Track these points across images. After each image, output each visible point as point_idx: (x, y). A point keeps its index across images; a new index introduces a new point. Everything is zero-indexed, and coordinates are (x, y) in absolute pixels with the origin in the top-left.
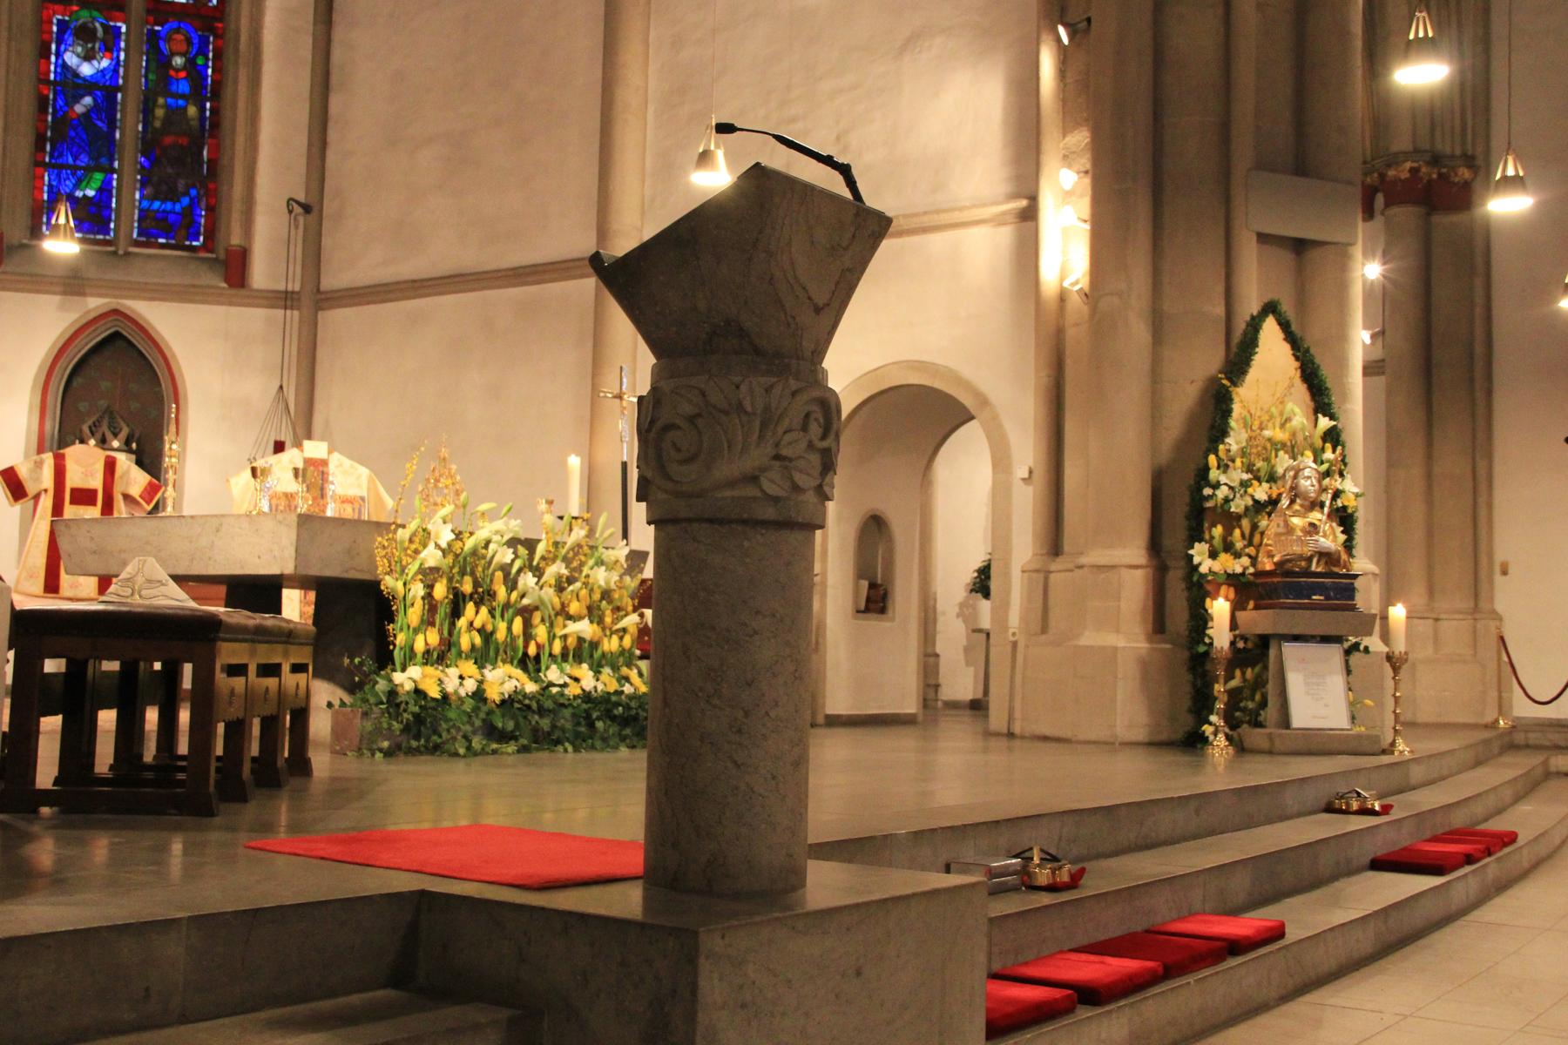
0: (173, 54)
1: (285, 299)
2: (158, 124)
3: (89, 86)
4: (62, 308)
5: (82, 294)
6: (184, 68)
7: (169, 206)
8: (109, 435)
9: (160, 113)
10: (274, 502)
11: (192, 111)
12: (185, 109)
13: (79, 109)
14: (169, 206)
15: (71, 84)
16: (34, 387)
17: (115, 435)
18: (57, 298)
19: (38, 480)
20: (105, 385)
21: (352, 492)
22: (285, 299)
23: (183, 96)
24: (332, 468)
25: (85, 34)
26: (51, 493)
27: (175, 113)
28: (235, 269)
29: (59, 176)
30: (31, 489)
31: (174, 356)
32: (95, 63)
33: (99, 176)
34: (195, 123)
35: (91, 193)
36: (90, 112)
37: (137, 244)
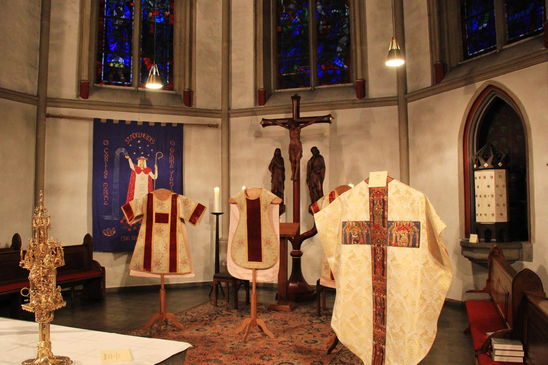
4: (466, 93)
5: (473, 82)
8: (482, 161)
10: (348, 231)
17: (486, 160)
18: (463, 88)
21: (408, 218)
33: (487, 15)
35: (485, 25)
37: (510, 42)
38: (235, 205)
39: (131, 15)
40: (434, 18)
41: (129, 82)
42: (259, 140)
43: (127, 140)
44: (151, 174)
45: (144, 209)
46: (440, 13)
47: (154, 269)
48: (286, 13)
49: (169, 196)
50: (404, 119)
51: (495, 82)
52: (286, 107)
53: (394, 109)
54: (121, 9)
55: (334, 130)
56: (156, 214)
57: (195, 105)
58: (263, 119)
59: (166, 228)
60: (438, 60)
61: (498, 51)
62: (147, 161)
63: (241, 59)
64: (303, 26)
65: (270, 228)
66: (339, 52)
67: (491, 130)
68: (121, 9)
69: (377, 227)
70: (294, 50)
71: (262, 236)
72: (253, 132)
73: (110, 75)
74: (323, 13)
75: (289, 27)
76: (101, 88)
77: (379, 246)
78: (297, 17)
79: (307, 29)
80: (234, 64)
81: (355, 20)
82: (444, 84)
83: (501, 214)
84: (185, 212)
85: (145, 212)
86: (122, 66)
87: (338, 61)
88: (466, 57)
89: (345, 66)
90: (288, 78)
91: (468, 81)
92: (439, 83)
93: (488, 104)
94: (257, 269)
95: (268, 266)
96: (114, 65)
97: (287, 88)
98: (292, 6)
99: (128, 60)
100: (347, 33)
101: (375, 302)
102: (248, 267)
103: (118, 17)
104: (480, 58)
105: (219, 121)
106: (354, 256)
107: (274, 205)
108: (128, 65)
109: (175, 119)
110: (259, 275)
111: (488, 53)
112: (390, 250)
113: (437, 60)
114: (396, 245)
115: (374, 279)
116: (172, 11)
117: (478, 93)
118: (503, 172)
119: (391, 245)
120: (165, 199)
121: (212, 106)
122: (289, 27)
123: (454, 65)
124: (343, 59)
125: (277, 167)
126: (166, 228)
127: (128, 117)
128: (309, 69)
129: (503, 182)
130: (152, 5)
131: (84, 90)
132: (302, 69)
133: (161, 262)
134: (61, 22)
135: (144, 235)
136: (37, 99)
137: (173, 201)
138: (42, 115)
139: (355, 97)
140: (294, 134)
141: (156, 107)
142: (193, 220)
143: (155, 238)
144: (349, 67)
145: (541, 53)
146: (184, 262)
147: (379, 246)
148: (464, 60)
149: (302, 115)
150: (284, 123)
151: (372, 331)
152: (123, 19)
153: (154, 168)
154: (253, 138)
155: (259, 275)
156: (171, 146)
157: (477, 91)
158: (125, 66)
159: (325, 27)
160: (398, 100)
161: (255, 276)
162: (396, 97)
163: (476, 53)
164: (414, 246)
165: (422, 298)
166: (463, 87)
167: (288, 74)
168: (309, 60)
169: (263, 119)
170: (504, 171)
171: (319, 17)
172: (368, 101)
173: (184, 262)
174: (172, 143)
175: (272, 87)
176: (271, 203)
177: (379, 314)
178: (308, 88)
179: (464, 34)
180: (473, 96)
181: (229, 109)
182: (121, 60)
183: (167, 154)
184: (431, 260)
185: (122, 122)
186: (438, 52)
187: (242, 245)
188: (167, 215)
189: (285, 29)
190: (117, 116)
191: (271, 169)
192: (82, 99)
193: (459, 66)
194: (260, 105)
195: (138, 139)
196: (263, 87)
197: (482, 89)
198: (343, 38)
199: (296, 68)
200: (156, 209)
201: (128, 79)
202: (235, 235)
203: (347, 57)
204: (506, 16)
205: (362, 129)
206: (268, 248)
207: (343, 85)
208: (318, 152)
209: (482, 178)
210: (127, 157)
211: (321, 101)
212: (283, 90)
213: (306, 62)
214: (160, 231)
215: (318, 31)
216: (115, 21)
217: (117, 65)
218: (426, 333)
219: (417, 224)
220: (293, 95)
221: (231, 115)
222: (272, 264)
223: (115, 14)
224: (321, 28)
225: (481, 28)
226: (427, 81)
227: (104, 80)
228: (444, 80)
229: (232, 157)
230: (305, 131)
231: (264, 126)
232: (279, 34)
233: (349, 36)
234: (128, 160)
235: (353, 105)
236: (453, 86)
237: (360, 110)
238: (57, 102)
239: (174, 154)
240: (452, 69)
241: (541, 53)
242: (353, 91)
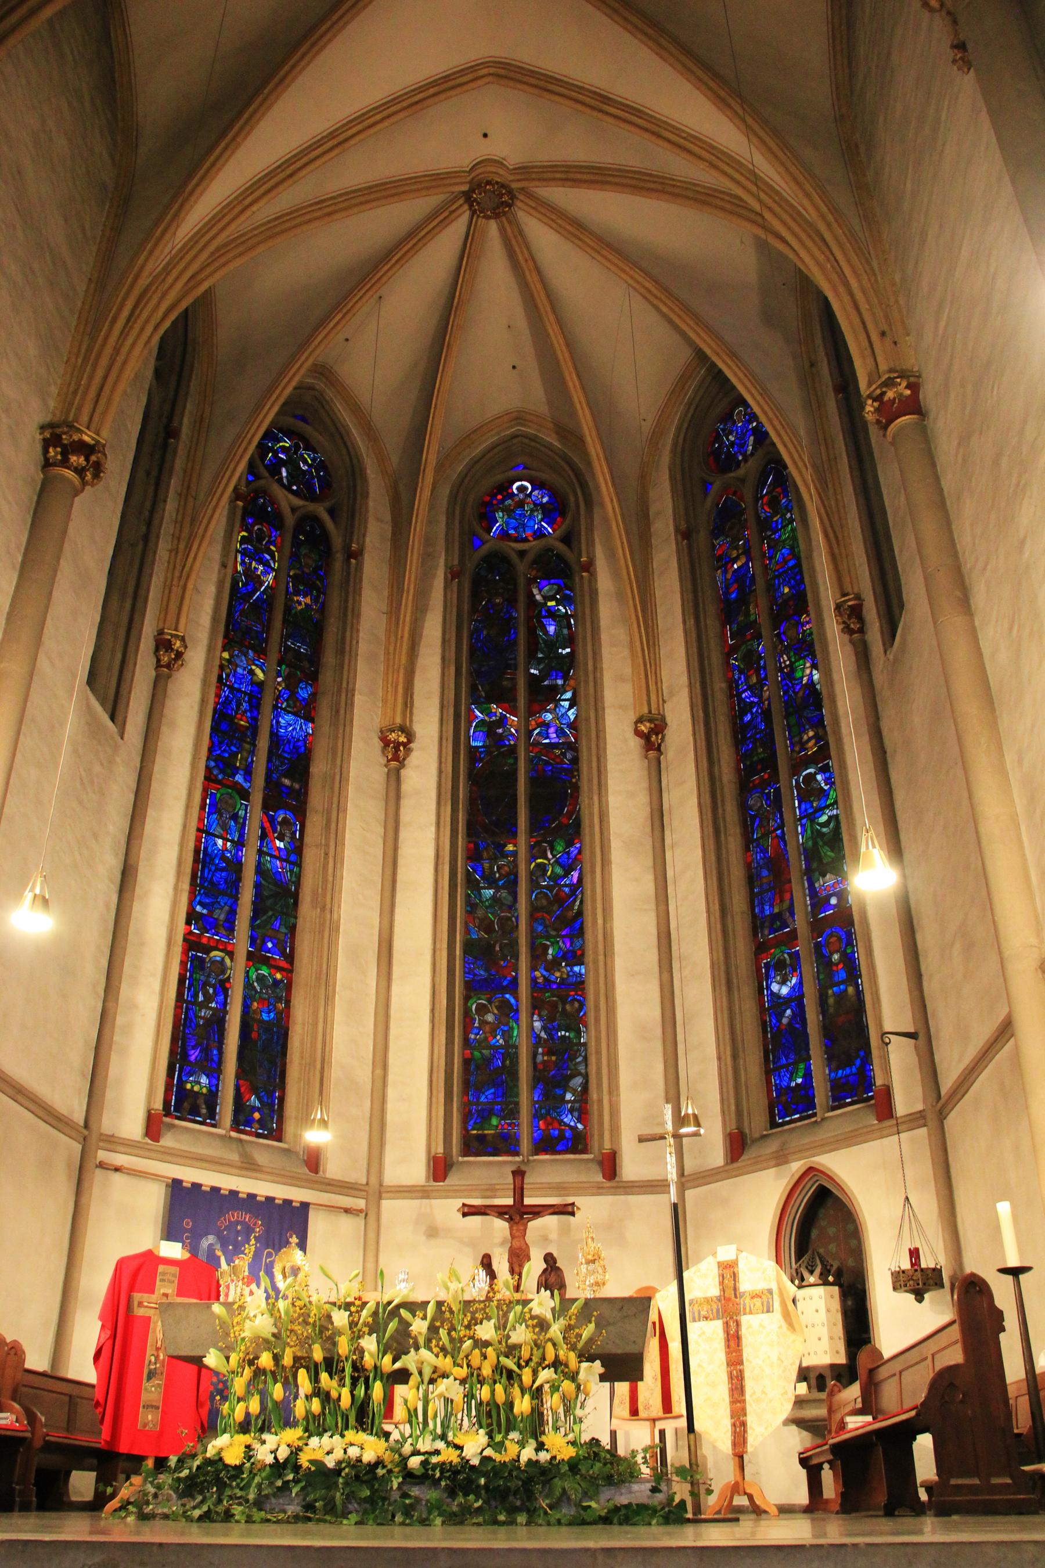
0: (832, 954)
1: (917, 1120)
2: (831, 1010)
3: (787, 1001)
6: (840, 961)
7: (848, 1071)
8: (806, 1274)
9: (831, 1001)
11: (851, 990)
12: (846, 990)
13: (785, 1021)
14: (848, 1071)
15: (778, 1003)
18: (772, 1171)
20: (831, 1231)
21: (761, 1286)
22: (917, 1120)
23: (843, 982)
24: (741, 1265)
25: (780, 965)
27: (841, 996)
28: (884, 1108)
29: (779, 1076)
31: (853, 1193)
32: (788, 983)
33: (802, 1066)
34: (854, 999)
35: (799, 1081)
36: (793, 1018)
37: (833, 1109)
39: (225, 1004)
40: (726, 1065)
41: (214, 1119)
43: (223, 1223)
44: (253, 1286)
46: (735, 1057)
48: (479, 1028)
52: (485, 1187)
54: (211, 991)
55: (565, 1230)
58: (464, 1205)
60: (734, 1127)
64: (510, 1052)
67: (814, 1233)
68: (211, 991)
69: (729, 1299)
70: (492, 1090)
73: (185, 1104)
74: (543, 1035)
75: (484, 1051)
76: (173, 1126)
77: (731, 1318)
78: (498, 1037)
79: (515, 1059)
80: (390, 1106)
81: (598, 1052)
82: (744, 1164)
83: (837, 1352)
86: (204, 1090)
88: (773, 1125)
89: (580, 1126)
90: (481, 1138)
91: (781, 1159)
96: (192, 1087)
98: (490, 1018)
99: (214, 1081)
100: (583, 1071)
101: (731, 1377)
103: (204, 1005)
104: (793, 1129)
106: (703, 1333)
108: (214, 1089)
109: (297, 1194)
111: (806, 1122)
112: (745, 1320)
113: (733, 1127)
114: (751, 1313)
115: (728, 1353)
116: (288, 1002)
119: (745, 1314)
122: (484, 1051)
123: (757, 1135)
124: (576, 1114)
127: (227, 1182)
129: (836, 1304)
130: (258, 988)
131: (153, 1127)
132: (505, 1126)
134: (133, 1007)
136: (86, 1132)
138: (90, 1165)
139: (600, 1178)
140: (518, 1230)
141: (269, 1170)
145: (873, 1128)
147: (731, 1318)
148: (771, 1128)
149: (527, 1201)
150: (501, 1212)
151: (728, 1410)
152: (211, 1008)
154: (424, 1238)
158: (210, 1091)
159: (546, 1058)
164: (768, 1311)
165: (779, 1359)
169: (464, 1205)
170: (837, 1288)
171: (537, 1040)
172: (621, 1184)
175: (454, 1150)
177: (736, 1388)
178: (517, 1159)
179: (769, 1092)
180: (789, 1182)
181: (381, 1185)
182: (204, 1080)
184: (785, 1326)
185: (216, 1190)
186: (733, 1116)
189: (477, 1054)
190: (208, 1178)
192: (149, 1141)
193: (764, 1137)
195: (238, 1223)
199: (494, 1121)
201: (212, 1114)
204: (827, 1072)
207: (577, 1156)
208: (555, 1261)
209: (807, 1299)
210: (219, 1253)
213: (513, 1113)
215: (535, 1064)
216: (200, 1010)
217: (196, 1088)
218: (786, 1393)
219: (770, 1291)
220: (514, 1168)
223: (201, 998)
224: (539, 1058)
225: (793, 1084)
226: (717, 1156)
227: (175, 1110)
228: (742, 1158)
230: (535, 1225)
231: (464, 1215)
232: (466, 1062)
233: (586, 1077)
234: (219, 1257)
235: (598, 1190)
236: (759, 1165)
237: (610, 1199)
238: (112, 1142)
240: (754, 1141)
241: (873, 1128)
242: (595, 1168)
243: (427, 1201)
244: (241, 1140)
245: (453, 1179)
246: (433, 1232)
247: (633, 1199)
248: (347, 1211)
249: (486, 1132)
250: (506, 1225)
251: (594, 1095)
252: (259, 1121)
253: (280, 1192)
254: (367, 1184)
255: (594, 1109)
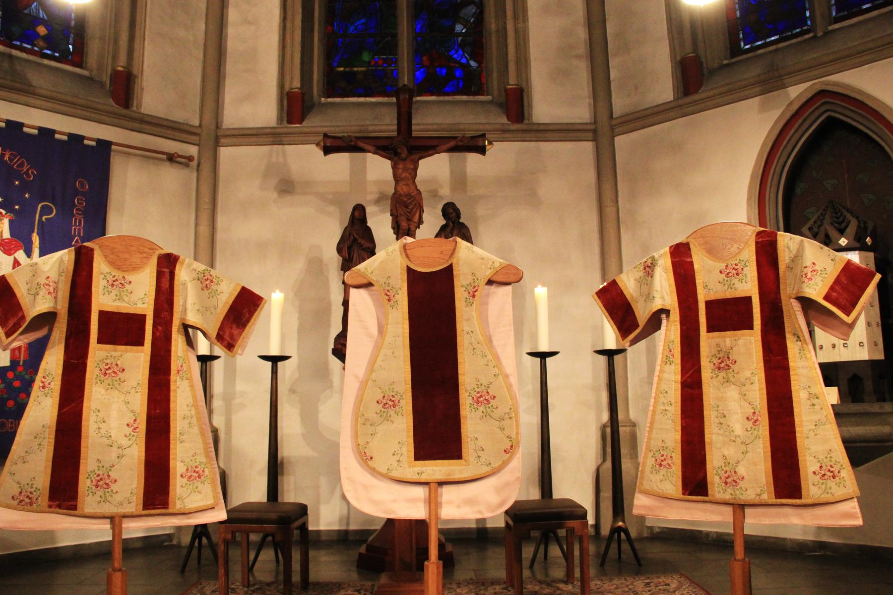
4: (763, 108)
5: (784, 87)
8: (833, 233)
16: (749, 198)
17: (842, 232)
19: (649, 297)
26: (675, 315)
30: (642, 314)
37: (837, 20)
38: (362, 292)
42: (288, 198)
44: (20, 255)
45: (60, 295)
47: (89, 501)
49: (148, 258)
50: (606, 168)
51: (836, 84)
53: (587, 147)
56: (104, 316)
57: (139, 106)
59: (136, 361)
61: (820, 34)
62: (11, 223)
63: (250, 23)
65: (488, 353)
66: (461, 34)
70: (363, 20)
71: (462, 379)
72: (274, 182)
84: (204, 310)
85: (63, 308)
87: (457, 51)
89: (473, 63)
90: (350, 77)
91: (771, 82)
92: (696, 91)
93: (810, 131)
94: (441, 484)
95: (485, 470)
97: (348, 97)
102: (416, 478)
105: (193, 150)
107: (493, 288)
110: (450, 502)
111: (807, 36)
117: (796, 107)
118: (871, 255)
120: (135, 269)
121: (178, 115)
125: (361, 246)
126: (136, 361)
128: (395, 61)
132: (380, 62)
133: (113, 475)
135: (56, 385)
137: (160, 275)
139: (504, 120)
140: (405, 169)
142: (227, 337)
143: (96, 394)
144: (479, 66)
146: (195, 475)
153: (31, 243)
155: (450, 502)
156: (76, 193)
157: (791, 103)
160: (595, 131)
161: (433, 502)
162: (591, 124)
163: (759, 43)
166: (757, 98)
167: (347, 69)
168: (396, 45)
173: (195, 475)
174: (81, 184)
176: (490, 282)
181: (218, 126)
183: (66, 209)
187: (391, 412)
188: (143, 318)
191: (345, 250)
194: (289, 122)
196: (299, 85)
197: (804, 100)
198: (470, 8)
199: (366, 57)
200: (103, 299)
202: (364, 384)
203: (476, 43)
205: (522, 187)
206: (486, 415)
207: (471, 98)
211: (429, 122)
212: (338, 100)
213: (391, 47)
214: (110, 371)
221: (222, 141)
222: (496, 464)
226: (663, 90)
229: (220, 236)
235: (505, 135)
239: (85, 213)
240: (712, 72)
243: (280, 147)
244: (10, 56)
245: (315, 123)
246: (287, 187)
247: (547, 147)
248: (171, 158)
249: (356, 69)
250: (388, 163)
251: (492, 24)
252: (46, 38)
253: (63, 125)
254: (200, 126)
255: (493, 43)
